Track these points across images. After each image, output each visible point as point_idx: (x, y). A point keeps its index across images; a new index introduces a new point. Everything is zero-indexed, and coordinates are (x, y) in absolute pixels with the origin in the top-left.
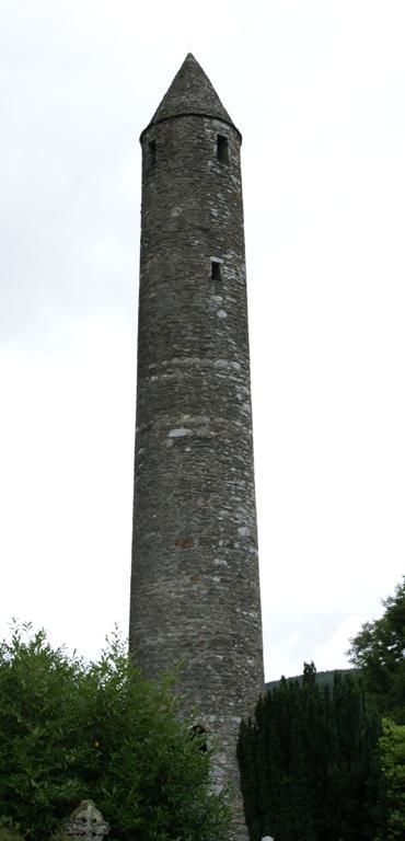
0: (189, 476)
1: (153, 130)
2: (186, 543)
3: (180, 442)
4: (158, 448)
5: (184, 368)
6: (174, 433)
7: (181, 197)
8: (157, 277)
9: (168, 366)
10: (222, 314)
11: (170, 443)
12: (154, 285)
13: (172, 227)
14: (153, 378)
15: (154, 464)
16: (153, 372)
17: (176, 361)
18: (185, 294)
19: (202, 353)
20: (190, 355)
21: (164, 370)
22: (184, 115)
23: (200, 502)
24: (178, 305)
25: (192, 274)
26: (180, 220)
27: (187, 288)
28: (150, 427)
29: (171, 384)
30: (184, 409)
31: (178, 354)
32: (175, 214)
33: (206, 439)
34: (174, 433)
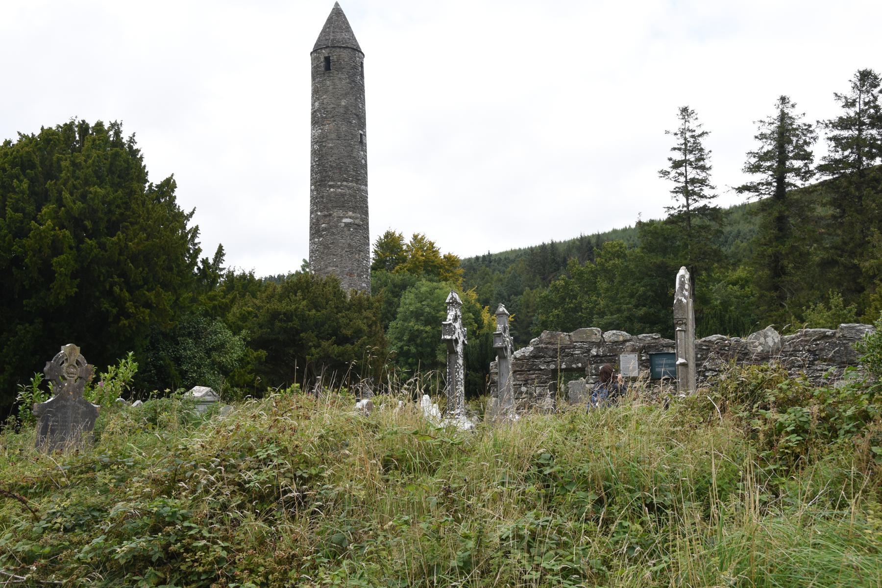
0: (353, 243)
1: (328, 50)
2: (351, 274)
3: (347, 225)
4: (336, 227)
5: (349, 188)
6: (345, 220)
7: (346, 94)
8: (333, 136)
9: (341, 185)
10: (363, 161)
11: (343, 225)
12: (332, 139)
13: (342, 110)
14: (332, 190)
15: (333, 234)
16: (331, 186)
17: (345, 183)
18: (349, 148)
19: (357, 181)
20: (352, 181)
21: (339, 187)
22: (347, 47)
23: (357, 256)
24: (346, 154)
25: (352, 139)
26: (346, 107)
27: (350, 145)
28: (330, 215)
29: (343, 195)
30: (349, 209)
31: (346, 180)
32: (343, 104)
33: (359, 226)
34: (345, 220)
